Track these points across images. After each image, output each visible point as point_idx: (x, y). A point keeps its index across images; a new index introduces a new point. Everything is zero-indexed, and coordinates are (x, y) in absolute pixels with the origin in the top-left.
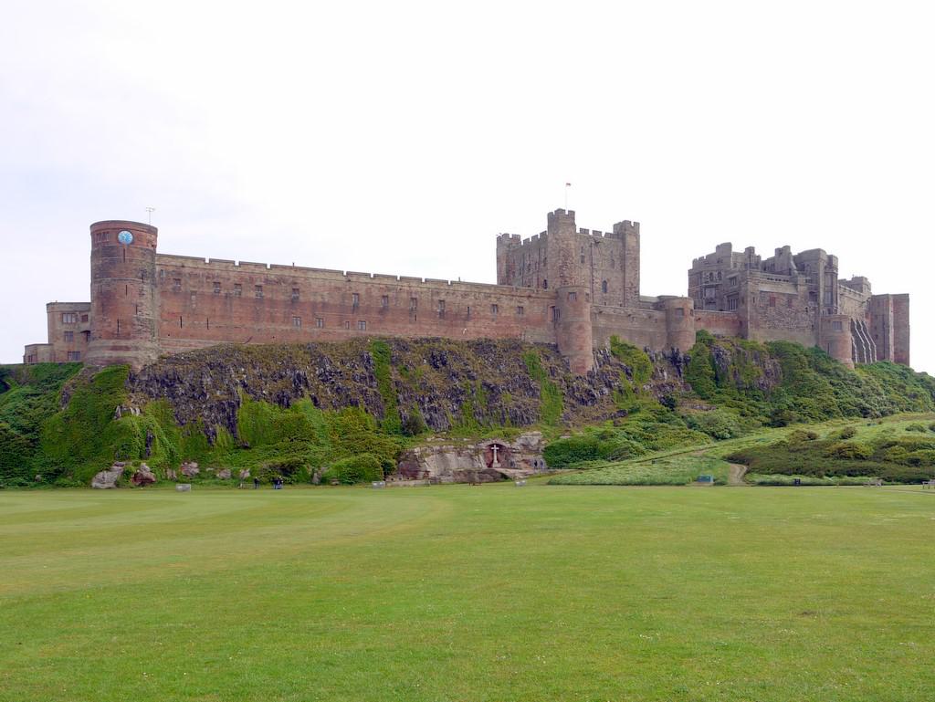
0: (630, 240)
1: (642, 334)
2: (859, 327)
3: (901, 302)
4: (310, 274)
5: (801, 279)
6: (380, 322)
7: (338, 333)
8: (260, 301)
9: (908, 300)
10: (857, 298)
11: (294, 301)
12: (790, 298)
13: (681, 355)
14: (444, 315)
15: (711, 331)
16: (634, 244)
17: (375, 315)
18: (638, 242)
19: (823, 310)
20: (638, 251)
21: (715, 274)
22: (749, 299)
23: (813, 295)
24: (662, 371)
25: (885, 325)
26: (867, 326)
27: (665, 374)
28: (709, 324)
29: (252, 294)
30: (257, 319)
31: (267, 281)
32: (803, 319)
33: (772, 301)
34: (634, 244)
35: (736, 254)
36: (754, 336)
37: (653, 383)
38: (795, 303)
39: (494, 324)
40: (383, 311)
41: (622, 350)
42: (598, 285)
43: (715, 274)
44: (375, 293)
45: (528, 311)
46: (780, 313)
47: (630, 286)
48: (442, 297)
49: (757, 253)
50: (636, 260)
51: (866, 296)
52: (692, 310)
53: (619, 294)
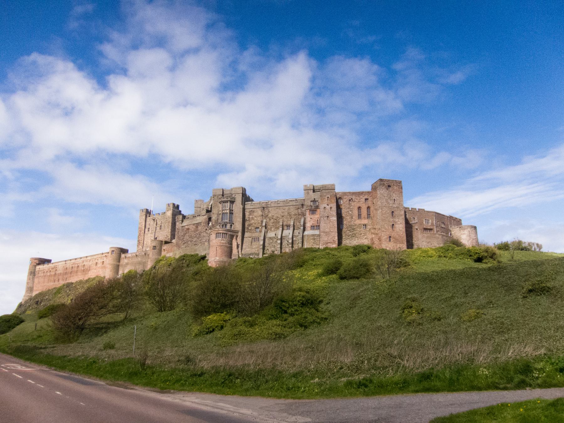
1: (140, 263)
4: (60, 263)
6: (70, 277)
7: (62, 283)
8: (50, 276)
11: (55, 274)
14: (86, 271)
17: (69, 275)
29: (49, 274)
30: (48, 282)
31: (52, 269)
32: (204, 236)
39: (95, 271)
40: (71, 273)
44: (71, 266)
45: (105, 263)
48: (85, 263)
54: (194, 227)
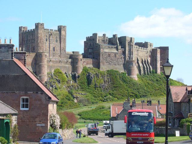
0: (63, 32)
2: (145, 61)
3: (165, 50)
5: (120, 47)
9: (168, 49)
10: (145, 50)
12: (115, 54)
13: (77, 75)
15: (88, 66)
16: (64, 34)
18: (65, 33)
19: (127, 58)
20: (65, 36)
21: (92, 44)
22: (101, 55)
23: (124, 53)
24: (70, 81)
25: (156, 60)
26: (149, 61)
27: (71, 82)
28: (87, 64)
33: (109, 55)
34: (64, 34)
35: (99, 37)
36: (102, 69)
37: (67, 85)
38: (117, 56)
41: (58, 73)
42: (51, 49)
43: (92, 44)
46: (112, 59)
47: (63, 48)
49: (107, 36)
50: (65, 39)
51: (149, 49)
52: (81, 59)
53: (59, 52)
54: (114, 54)
